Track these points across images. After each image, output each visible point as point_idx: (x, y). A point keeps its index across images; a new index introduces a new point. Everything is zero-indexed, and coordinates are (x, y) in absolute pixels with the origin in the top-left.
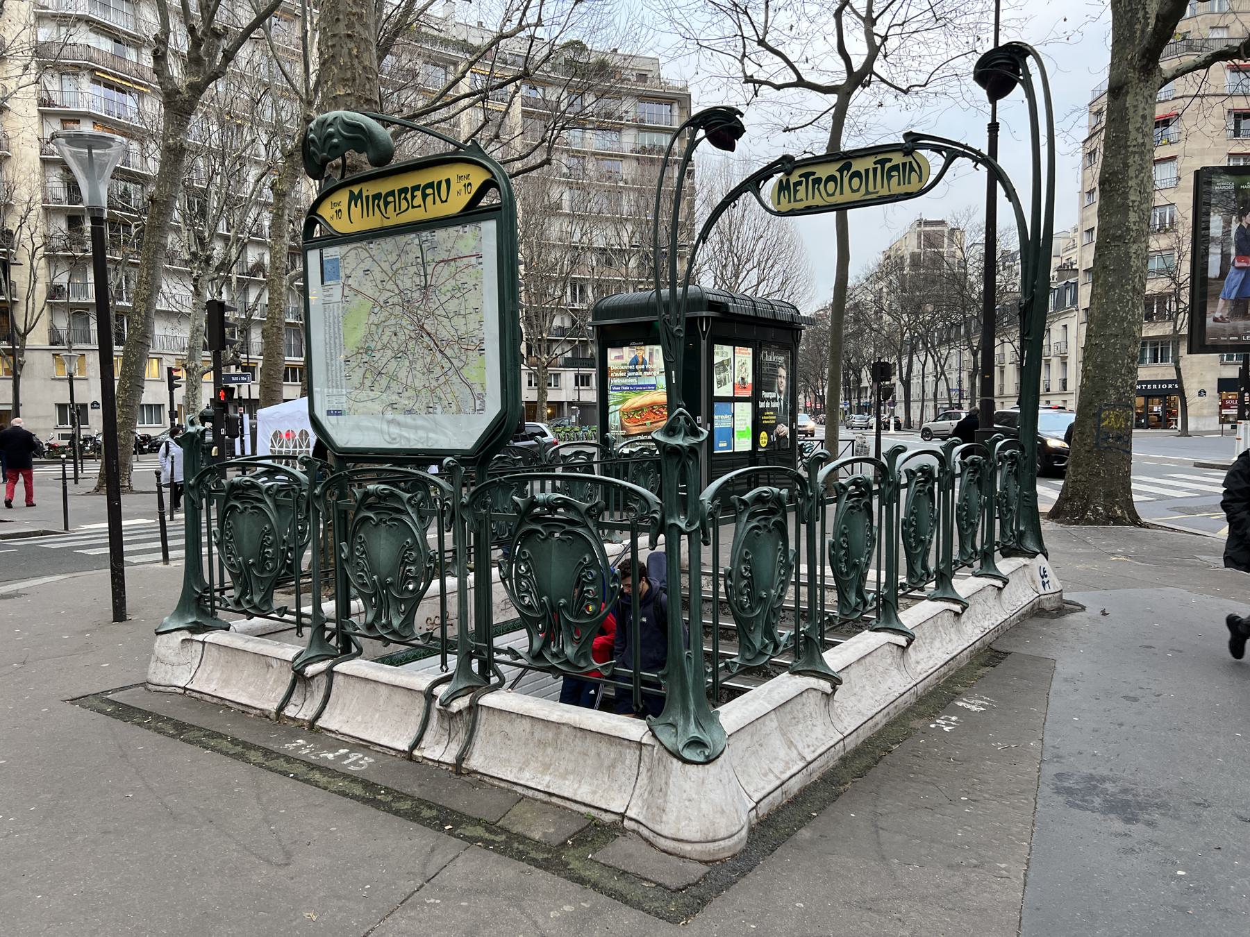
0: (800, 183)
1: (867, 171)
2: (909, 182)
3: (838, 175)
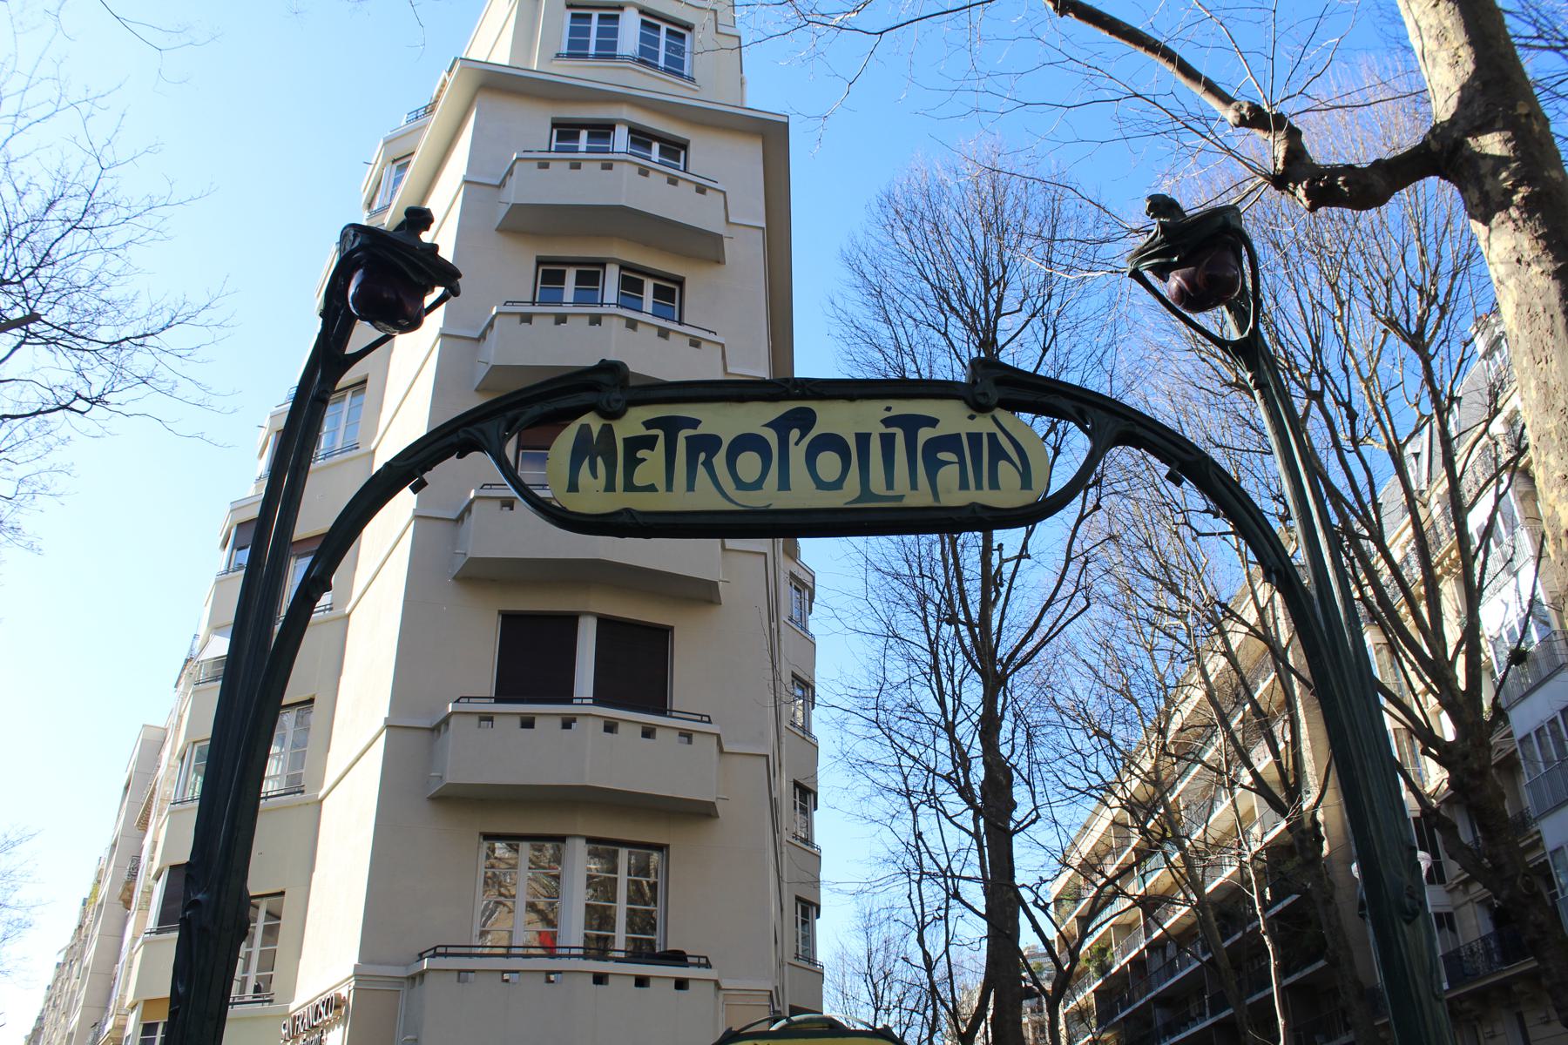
0: (649, 443)
1: (863, 440)
2: (994, 484)
3: (772, 437)
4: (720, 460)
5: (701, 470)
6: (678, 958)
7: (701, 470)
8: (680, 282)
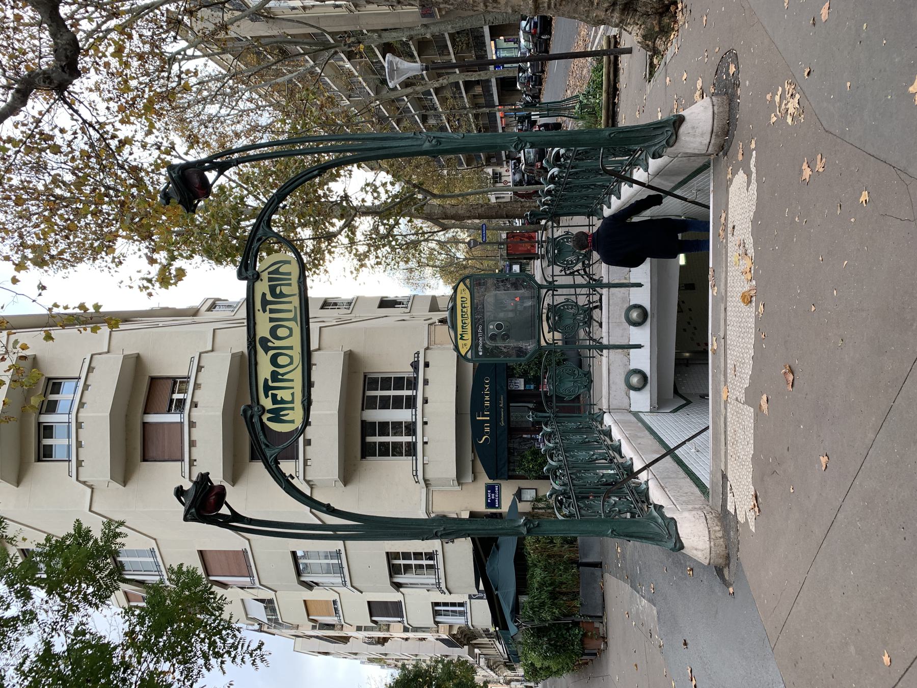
0: (274, 396)
1: (271, 320)
2: (289, 274)
3: (271, 353)
4: (281, 371)
5: (285, 377)
6: (415, 365)
7: (285, 377)
8: (49, 379)
